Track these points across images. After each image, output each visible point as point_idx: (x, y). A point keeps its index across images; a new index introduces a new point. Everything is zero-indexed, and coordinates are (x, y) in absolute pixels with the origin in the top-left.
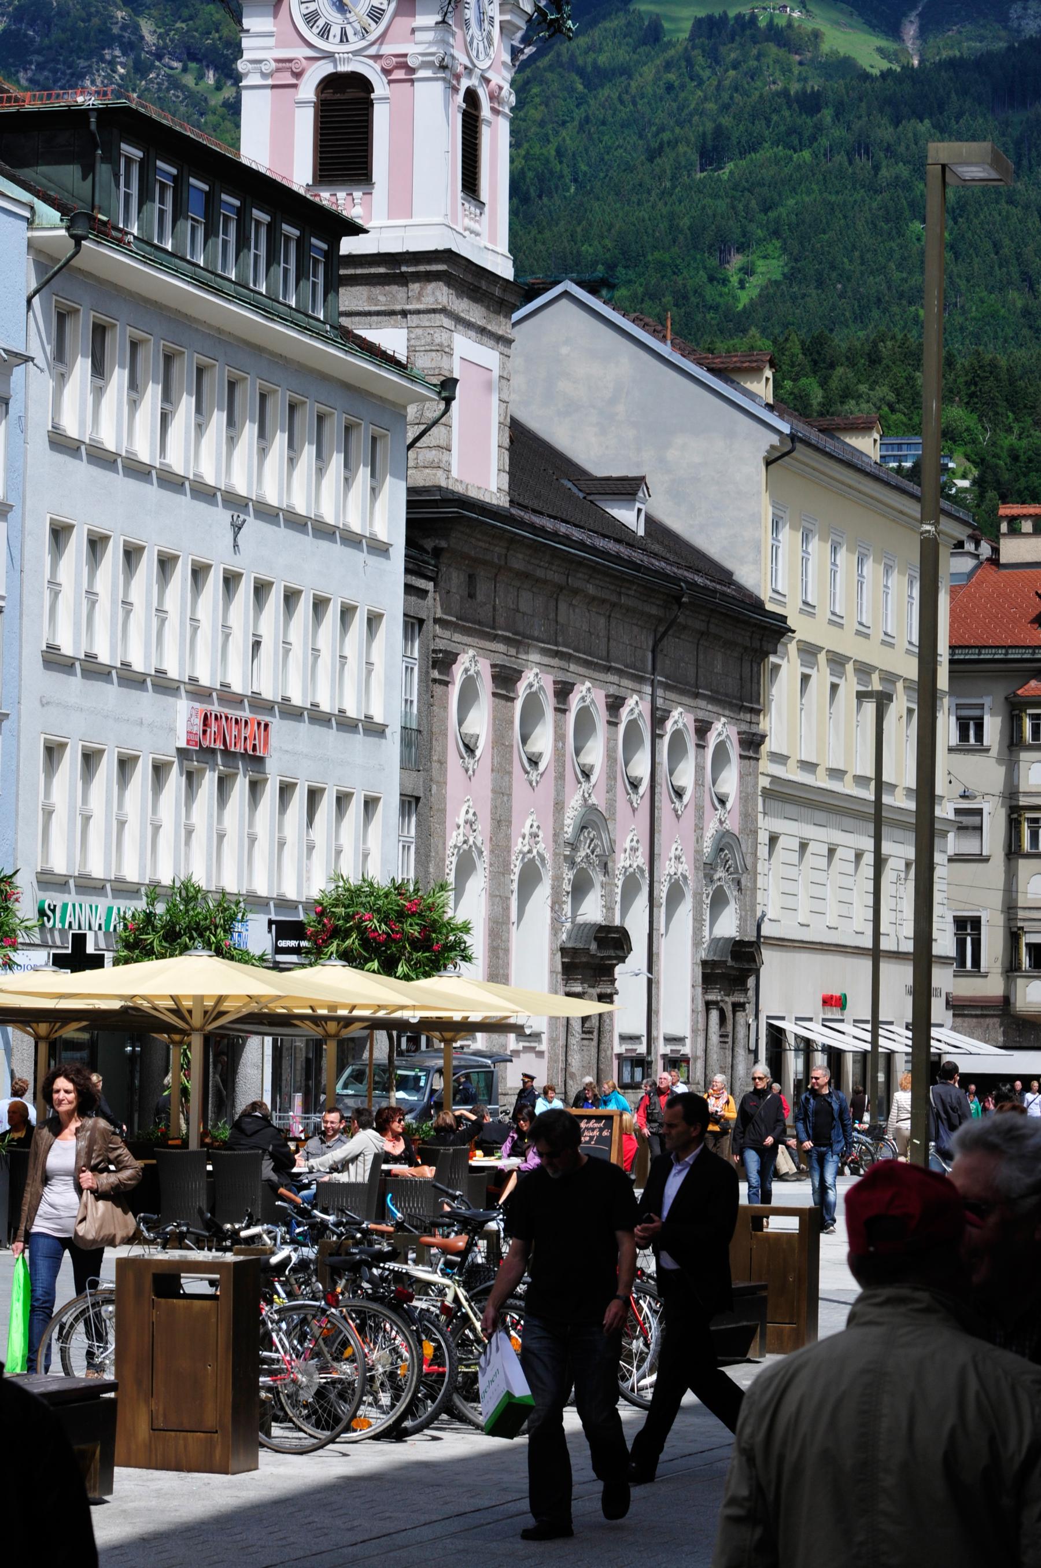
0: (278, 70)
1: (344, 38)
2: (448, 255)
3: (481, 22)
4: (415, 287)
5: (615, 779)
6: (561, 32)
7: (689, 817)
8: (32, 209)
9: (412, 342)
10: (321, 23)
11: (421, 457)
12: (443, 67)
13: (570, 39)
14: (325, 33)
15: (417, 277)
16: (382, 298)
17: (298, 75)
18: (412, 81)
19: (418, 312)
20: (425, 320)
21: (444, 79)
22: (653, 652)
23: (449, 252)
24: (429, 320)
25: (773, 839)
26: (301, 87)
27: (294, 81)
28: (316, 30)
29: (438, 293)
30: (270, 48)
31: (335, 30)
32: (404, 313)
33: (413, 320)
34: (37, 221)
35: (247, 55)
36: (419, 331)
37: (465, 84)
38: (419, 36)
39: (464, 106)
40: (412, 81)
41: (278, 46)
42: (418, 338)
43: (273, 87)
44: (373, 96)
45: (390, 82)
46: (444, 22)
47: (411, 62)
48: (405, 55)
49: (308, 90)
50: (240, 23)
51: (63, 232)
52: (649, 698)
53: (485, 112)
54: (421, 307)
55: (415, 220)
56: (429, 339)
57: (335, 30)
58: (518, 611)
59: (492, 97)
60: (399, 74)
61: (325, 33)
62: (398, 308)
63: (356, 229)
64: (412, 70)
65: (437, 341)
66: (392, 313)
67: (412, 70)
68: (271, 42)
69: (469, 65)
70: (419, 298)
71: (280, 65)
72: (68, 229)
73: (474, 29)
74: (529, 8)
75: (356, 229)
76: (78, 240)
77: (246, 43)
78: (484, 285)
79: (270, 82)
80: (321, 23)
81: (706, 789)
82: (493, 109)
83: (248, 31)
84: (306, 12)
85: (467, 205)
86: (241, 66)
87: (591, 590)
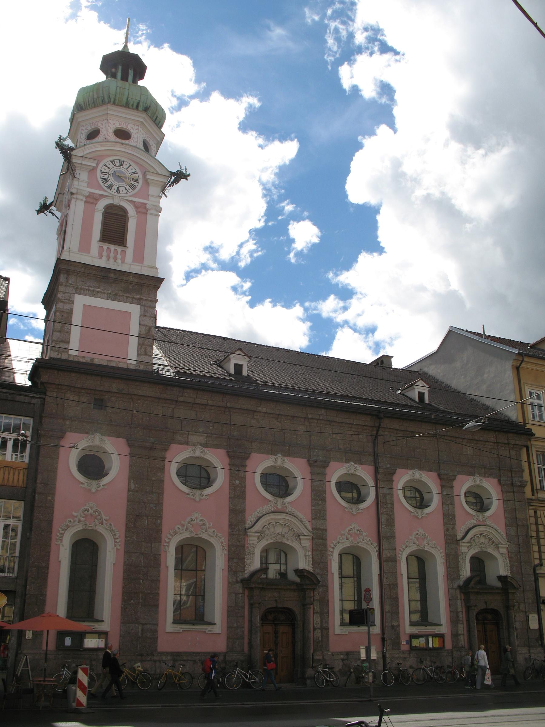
10: (109, 183)
31: (115, 187)
61: (110, 187)
64: (147, 210)
80: (109, 183)
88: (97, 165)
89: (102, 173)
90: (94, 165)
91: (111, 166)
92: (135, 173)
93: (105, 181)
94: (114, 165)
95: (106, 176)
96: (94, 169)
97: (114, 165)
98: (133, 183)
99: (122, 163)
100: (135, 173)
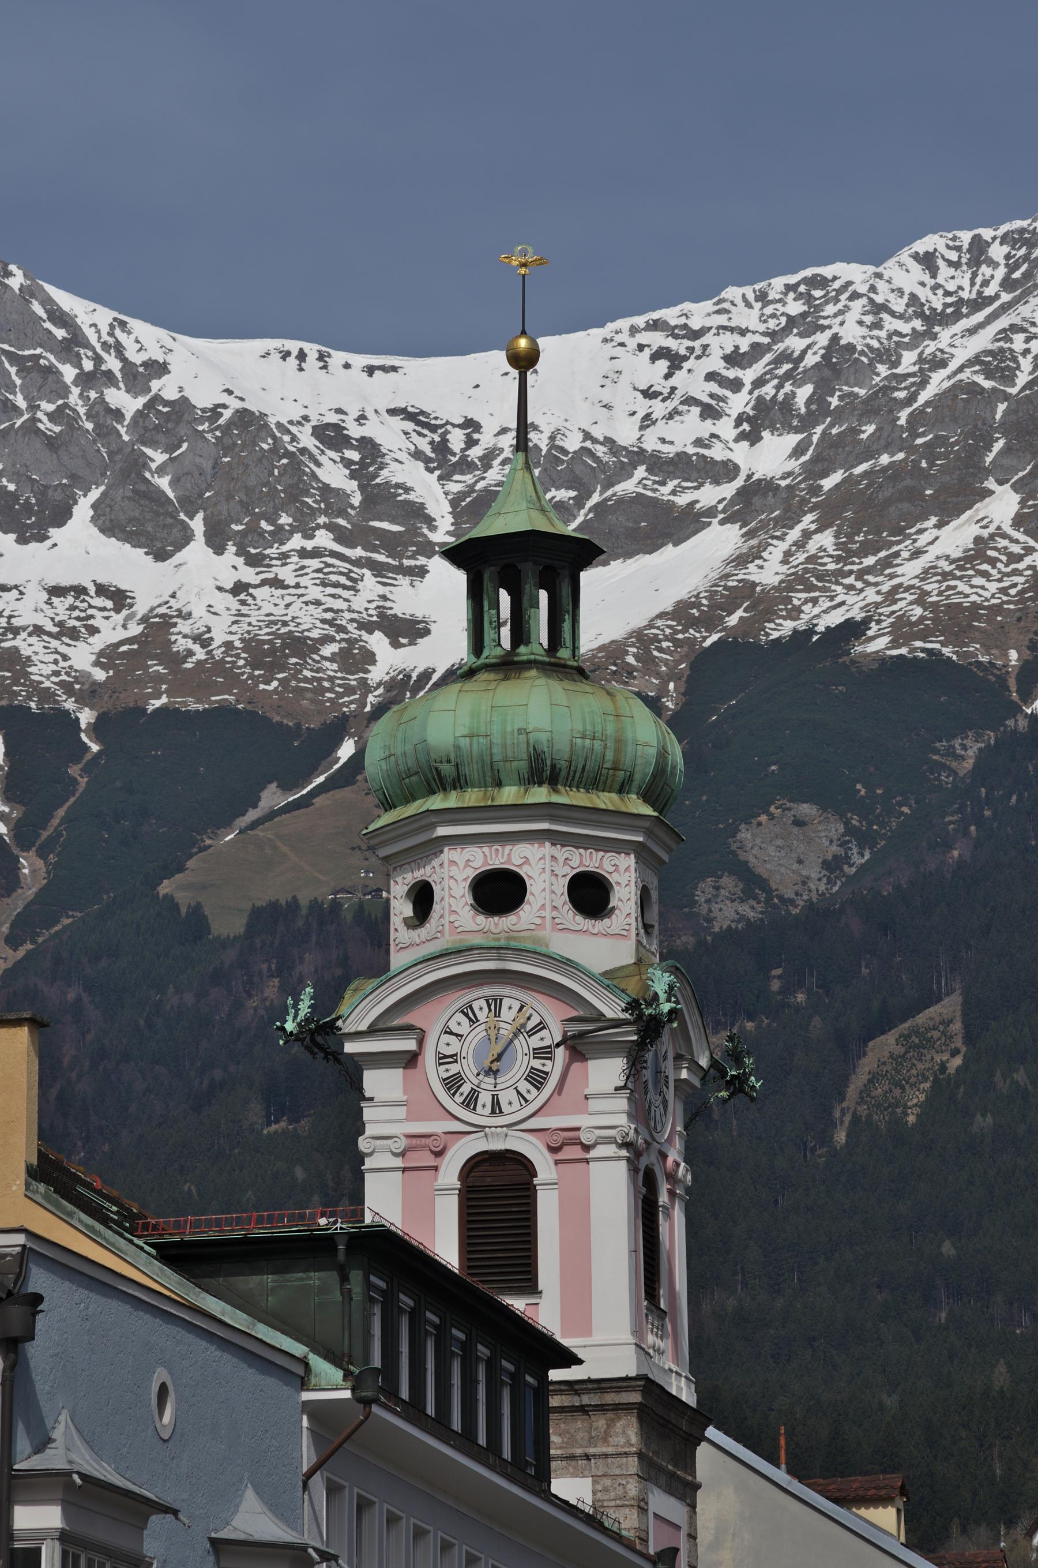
1: (496, 1108)
3: (656, 1082)
4: (600, 1422)
6: (741, 1090)
8: (307, 1365)
9: (599, 1495)
10: (466, 1089)
13: (752, 1099)
14: (471, 1102)
15: (602, 1408)
17: (439, 1154)
18: (587, 1161)
19: (606, 1456)
20: (614, 1467)
24: (620, 1466)
26: (442, 1171)
27: (431, 1161)
28: (459, 1099)
30: (400, 1121)
31: (485, 1098)
32: (587, 1457)
33: (598, 1466)
34: (313, 1381)
35: (370, 1130)
36: (608, 1482)
38: (593, 1105)
40: (587, 1161)
41: (408, 1120)
42: (605, 1490)
43: (404, 1170)
44: (536, 1181)
45: (557, 1162)
47: (586, 1138)
48: (578, 1129)
49: (450, 1173)
50: (360, 1089)
51: (347, 1394)
53: (663, 1198)
54: (610, 1450)
55: (597, 1338)
56: (620, 1492)
57: (485, 1098)
60: (568, 1153)
61: (471, 1102)
62: (579, 1451)
63: (569, 1359)
64: (587, 1148)
66: (572, 1457)
67: (587, 1148)
68: (401, 1112)
69: (649, 1139)
70: (605, 1440)
71: (414, 1141)
72: (353, 1390)
74: (704, 1062)
75: (569, 1359)
76: (367, 1402)
77: (369, 1113)
79: (398, 1162)
80: (466, 1089)
83: (371, 1099)
84: (446, 1075)
86: (363, 1144)
88: (421, 1043)
89: (443, 1059)
90: (410, 1045)
91: (465, 1028)
92: (541, 1026)
93: (453, 1084)
94: (473, 1021)
95: (454, 1069)
97: (473, 1021)
98: (537, 1064)
99: (495, 1005)
100: (541, 1026)
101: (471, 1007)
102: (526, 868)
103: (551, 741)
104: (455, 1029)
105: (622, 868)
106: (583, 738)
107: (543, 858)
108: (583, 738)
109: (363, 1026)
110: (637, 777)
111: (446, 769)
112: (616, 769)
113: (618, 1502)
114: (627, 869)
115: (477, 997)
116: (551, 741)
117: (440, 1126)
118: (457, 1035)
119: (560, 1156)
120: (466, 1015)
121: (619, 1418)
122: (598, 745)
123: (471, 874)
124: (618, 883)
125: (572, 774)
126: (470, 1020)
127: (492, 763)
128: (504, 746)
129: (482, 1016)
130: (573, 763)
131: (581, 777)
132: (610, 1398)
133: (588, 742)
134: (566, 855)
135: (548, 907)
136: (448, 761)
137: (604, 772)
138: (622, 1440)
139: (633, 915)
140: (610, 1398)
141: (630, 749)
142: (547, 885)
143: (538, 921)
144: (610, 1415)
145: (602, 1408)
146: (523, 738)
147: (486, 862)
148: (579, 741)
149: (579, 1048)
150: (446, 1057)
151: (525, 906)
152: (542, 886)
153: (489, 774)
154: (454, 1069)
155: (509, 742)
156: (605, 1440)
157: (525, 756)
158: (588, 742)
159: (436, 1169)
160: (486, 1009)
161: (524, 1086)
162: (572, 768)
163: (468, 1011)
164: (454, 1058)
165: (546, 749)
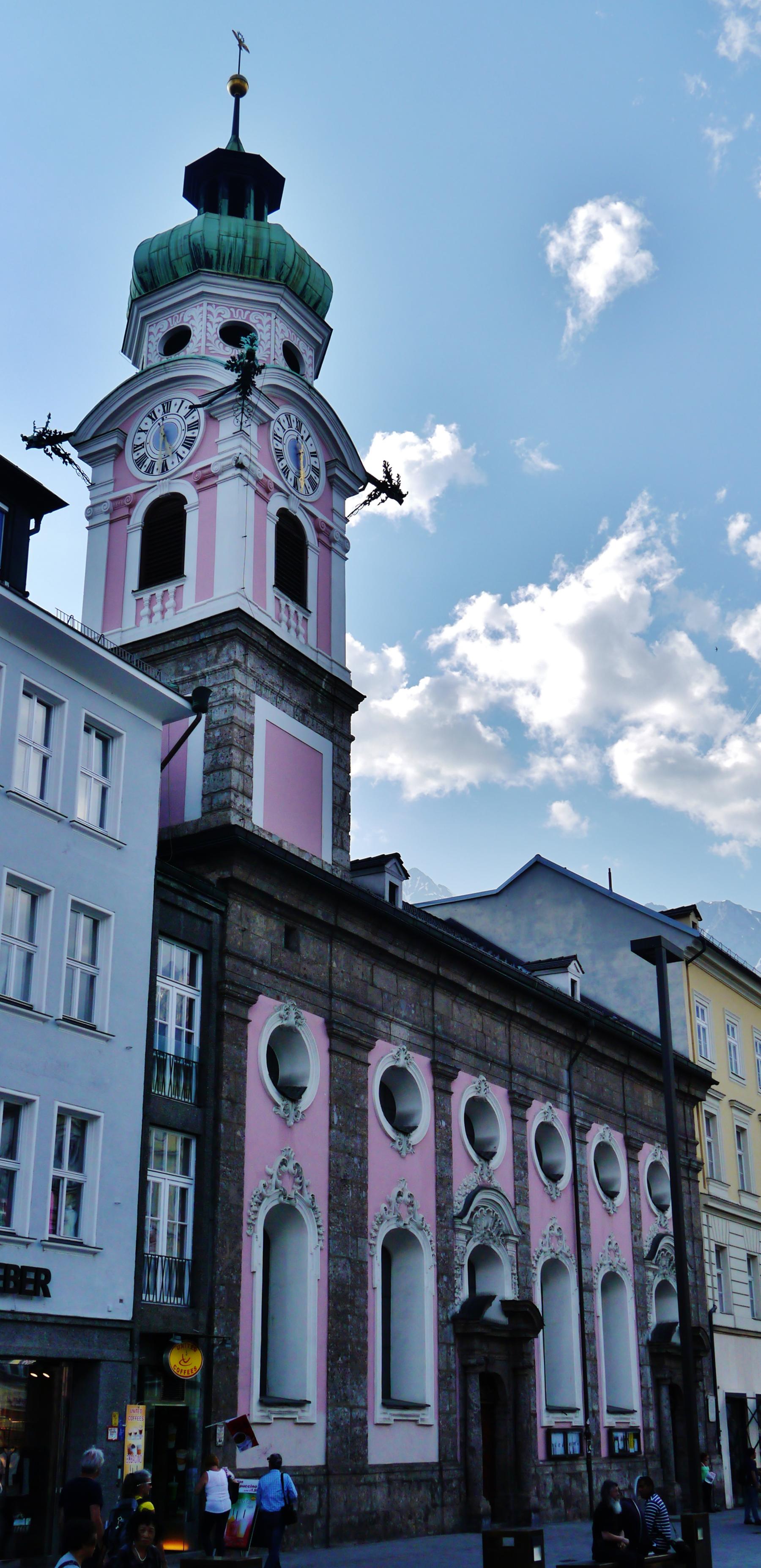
0: (115, 509)
2: (238, 614)
5: (526, 1169)
7: (623, 1219)
10: (148, 462)
11: (215, 801)
12: (240, 466)
15: (213, 639)
16: (186, 669)
19: (215, 671)
21: (241, 476)
22: (569, 1070)
23: (238, 610)
24: (224, 677)
25: (720, 1249)
28: (143, 469)
29: (232, 653)
31: (158, 465)
37: (277, 502)
38: (221, 448)
39: (277, 519)
40: (215, 485)
43: (111, 522)
44: (186, 507)
45: (199, 491)
46: (241, 430)
47: (213, 470)
48: (209, 466)
49: (138, 516)
52: (566, 1108)
56: (223, 694)
58: (373, 985)
59: (318, 530)
64: (215, 476)
65: (230, 694)
68: (111, 487)
73: (288, 461)
78: (301, 669)
79: (107, 517)
80: (148, 462)
81: (642, 1196)
82: (319, 540)
85: (283, 603)
87: (474, 988)
88: (124, 441)
89: (136, 448)
90: (114, 441)
93: (139, 463)
95: (142, 452)
96: (119, 451)
99: (166, 406)
101: (154, 412)
102: (192, 322)
103: (203, 238)
104: (144, 427)
105: (264, 323)
106: (229, 236)
107: (202, 313)
108: (229, 236)
109: (88, 437)
110: (274, 264)
111: (146, 276)
112: (255, 257)
113: (222, 702)
114: (269, 323)
115: (156, 404)
116: (203, 238)
117: (131, 490)
118: (144, 431)
119: (202, 486)
120: (150, 417)
121: (225, 644)
122: (240, 241)
123: (161, 335)
124: (261, 330)
125: (221, 260)
126: (153, 419)
127: (171, 262)
128: (176, 249)
129: (159, 415)
130: (222, 252)
131: (229, 262)
132: (218, 630)
133: (232, 239)
134: (220, 311)
135: (204, 340)
136: (146, 270)
137: (247, 259)
138: (226, 658)
139: (272, 350)
140: (218, 630)
141: (265, 245)
142: (204, 328)
143: (196, 350)
144: (219, 643)
145: (213, 639)
146: (187, 240)
147: (169, 326)
148: (225, 238)
149: (212, 413)
150: (138, 446)
151: (190, 344)
152: (199, 328)
153: (170, 271)
154: (142, 452)
155: (179, 245)
156: (216, 662)
157: (188, 251)
158: (232, 239)
159: (129, 516)
160: (162, 410)
161: (181, 450)
162: (222, 256)
163: (152, 416)
164: (142, 445)
165: (200, 242)
